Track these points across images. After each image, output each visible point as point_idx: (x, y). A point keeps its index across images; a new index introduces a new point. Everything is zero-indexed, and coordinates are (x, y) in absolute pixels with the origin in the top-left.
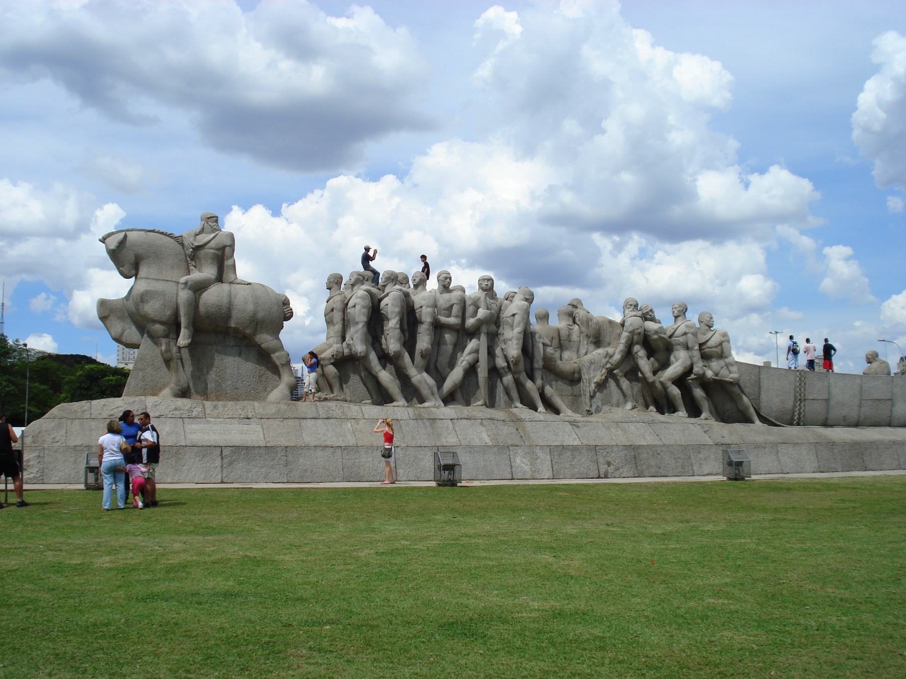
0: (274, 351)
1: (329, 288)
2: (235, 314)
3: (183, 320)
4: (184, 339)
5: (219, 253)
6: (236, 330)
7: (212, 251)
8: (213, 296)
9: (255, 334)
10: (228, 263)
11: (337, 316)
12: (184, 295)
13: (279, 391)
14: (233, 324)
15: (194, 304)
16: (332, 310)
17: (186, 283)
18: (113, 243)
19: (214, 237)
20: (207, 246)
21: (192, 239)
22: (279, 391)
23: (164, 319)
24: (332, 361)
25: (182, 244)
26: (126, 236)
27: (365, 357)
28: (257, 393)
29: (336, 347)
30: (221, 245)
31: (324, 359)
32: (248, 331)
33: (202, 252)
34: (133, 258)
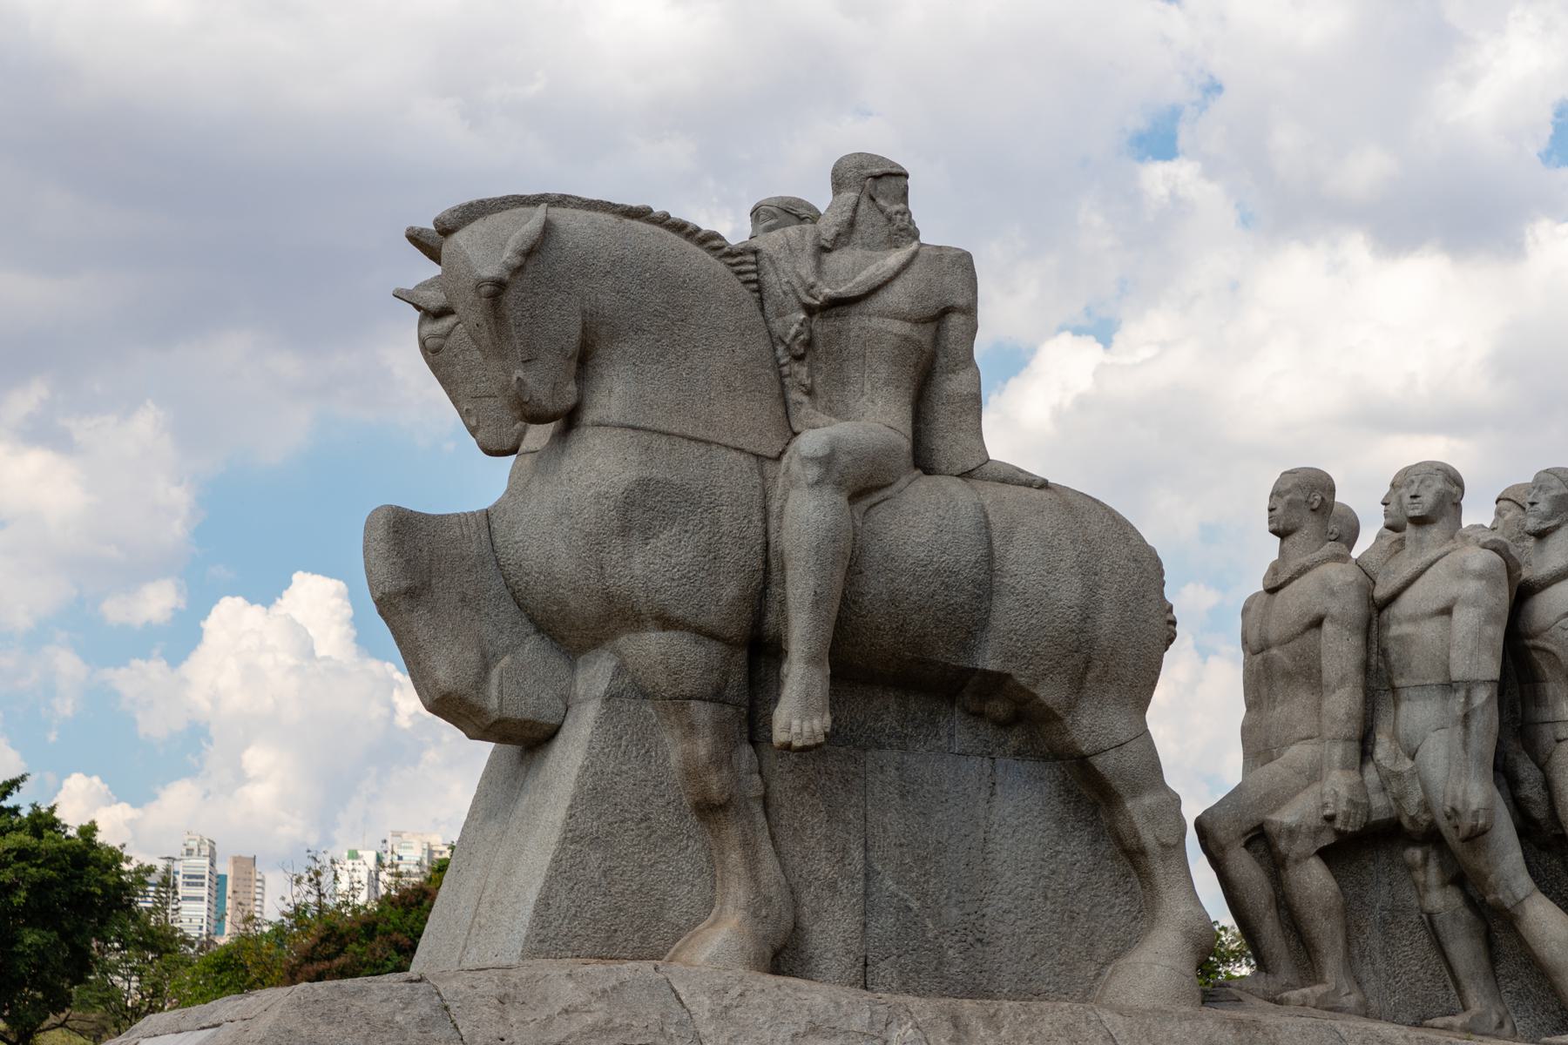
0: (1137, 791)
1: (1282, 533)
2: (1006, 613)
3: (802, 632)
4: (806, 712)
5: (923, 335)
6: (997, 683)
7: (899, 327)
8: (923, 520)
9: (1071, 706)
10: (954, 384)
11: (1339, 652)
12: (806, 515)
13: (1155, 965)
14: (989, 661)
15: (852, 563)
16: (1317, 623)
17: (827, 461)
18: (486, 253)
19: (905, 266)
20: (876, 304)
21: (806, 268)
22: (1155, 965)
23: (712, 618)
24: (1327, 839)
25: (759, 290)
26: (548, 229)
27: (1477, 837)
28: (1075, 964)
29: (1338, 786)
30: (932, 305)
31: (1292, 833)
32: (1050, 693)
33: (858, 323)
34: (575, 330)
